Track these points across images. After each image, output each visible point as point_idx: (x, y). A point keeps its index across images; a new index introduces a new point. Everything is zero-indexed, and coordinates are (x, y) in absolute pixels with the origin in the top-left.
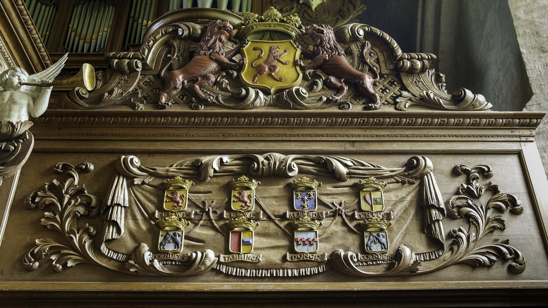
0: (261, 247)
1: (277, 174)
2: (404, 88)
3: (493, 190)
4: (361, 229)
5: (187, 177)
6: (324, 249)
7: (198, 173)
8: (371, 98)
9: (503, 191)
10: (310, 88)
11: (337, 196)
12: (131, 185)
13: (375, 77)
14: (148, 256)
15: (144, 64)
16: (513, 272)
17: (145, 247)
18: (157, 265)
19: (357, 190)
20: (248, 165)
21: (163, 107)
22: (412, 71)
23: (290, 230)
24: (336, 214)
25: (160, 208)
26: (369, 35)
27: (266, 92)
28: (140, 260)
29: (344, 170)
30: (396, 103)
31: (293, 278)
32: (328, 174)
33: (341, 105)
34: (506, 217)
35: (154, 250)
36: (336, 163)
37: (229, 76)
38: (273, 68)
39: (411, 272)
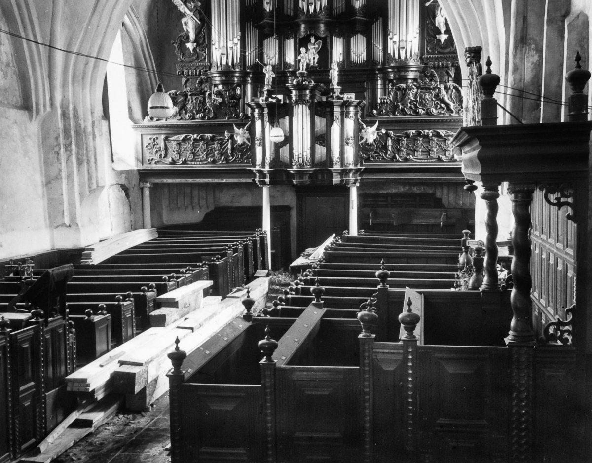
5: (405, 137)
7: (407, 136)
8: (452, 112)
10: (436, 109)
12: (391, 139)
13: (454, 103)
14: (398, 158)
15: (390, 100)
17: (396, 155)
18: (400, 160)
20: (419, 134)
21: (397, 115)
25: (399, 145)
27: (424, 110)
28: (396, 159)
29: (443, 135)
30: (459, 113)
31: (430, 162)
32: (438, 135)
33: (444, 114)
35: (398, 156)
36: (441, 134)
37: (414, 104)
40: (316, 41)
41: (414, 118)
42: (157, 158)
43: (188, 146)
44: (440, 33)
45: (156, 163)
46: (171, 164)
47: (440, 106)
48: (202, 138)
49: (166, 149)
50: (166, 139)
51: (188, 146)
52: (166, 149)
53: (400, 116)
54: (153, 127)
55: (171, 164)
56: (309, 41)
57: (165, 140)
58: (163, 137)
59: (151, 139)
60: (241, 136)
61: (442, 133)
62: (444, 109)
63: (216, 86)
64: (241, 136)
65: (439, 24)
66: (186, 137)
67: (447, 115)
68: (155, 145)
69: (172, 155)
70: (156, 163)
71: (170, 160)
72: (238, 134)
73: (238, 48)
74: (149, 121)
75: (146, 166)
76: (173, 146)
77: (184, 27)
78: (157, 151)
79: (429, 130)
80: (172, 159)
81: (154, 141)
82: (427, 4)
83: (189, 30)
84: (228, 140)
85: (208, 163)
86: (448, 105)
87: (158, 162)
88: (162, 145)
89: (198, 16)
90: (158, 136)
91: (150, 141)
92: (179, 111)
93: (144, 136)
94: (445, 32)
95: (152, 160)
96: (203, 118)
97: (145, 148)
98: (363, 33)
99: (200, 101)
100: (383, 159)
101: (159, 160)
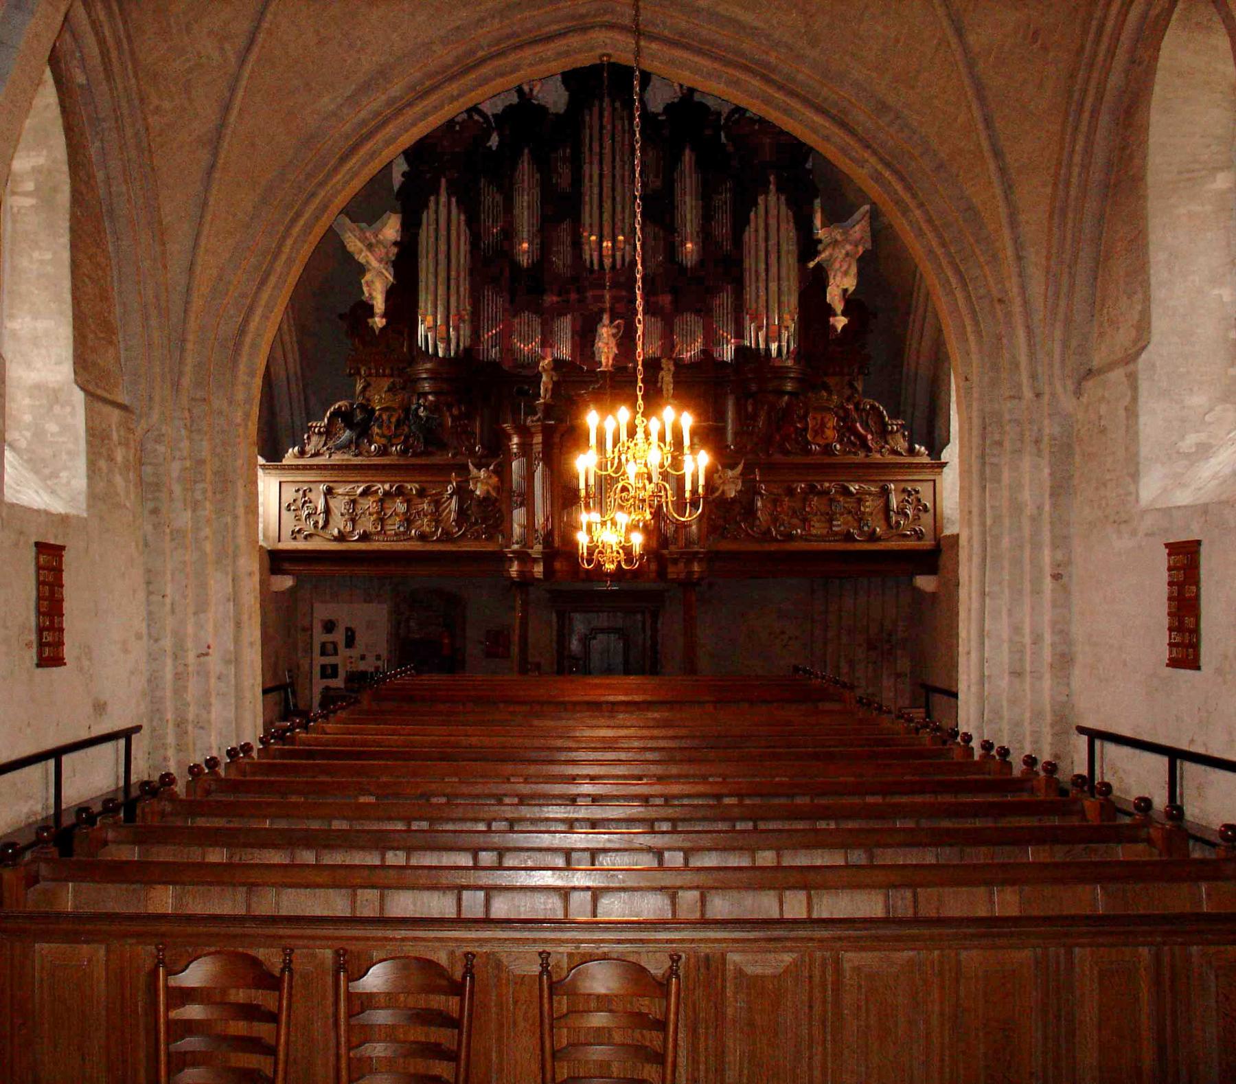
0: (818, 528)
1: (826, 492)
2: (886, 442)
3: (919, 500)
4: (861, 519)
6: (843, 528)
7: (790, 492)
8: (869, 450)
9: (923, 502)
11: (850, 503)
16: (919, 539)
19: (860, 501)
20: (812, 489)
22: (892, 432)
23: (831, 520)
24: (850, 512)
26: (872, 407)
32: (846, 492)
34: (921, 514)
38: (823, 432)
39: (879, 539)
40: (611, 322)
41: (799, 459)
42: (309, 527)
43: (369, 504)
44: (835, 315)
45: (306, 538)
46: (336, 539)
47: (849, 438)
48: (400, 492)
49: (327, 511)
50: (329, 492)
51: (369, 504)
52: (327, 511)
53: (778, 457)
54: (305, 467)
55: (336, 539)
56: (601, 319)
57: (325, 495)
58: (322, 487)
59: (297, 491)
60: (481, 483)
61: (854, 488)
62: (854, 444)
63: (425, 395)
64: (481, 483)
65: (832, 298)
66: (368, 488)
67: (862, 454)
68: (305, 502)
69: (339, 524)
70: (306, 538)
71: (336, 532)
72: (477, 480)
73: (465, 330)
74: (295, 457)
75: (288, 544)
76: (338, 505)
77: (365, 289)
78: (309, 515)
79: (830, 481)
80: (339, 531)
81: (304, 495)
82: (811, 265)
83: (374, 294)
84: (451, 495)
85: (411, 538)
86: (863, 439)
87: (311, 535)
88: (321, 506)
89: (392, 270)
90: (312, 486)
91: (294, 495)
92: (358, 438)
93: (283, 485)
94: (844, 314)
95: (299, 531)
96: (403, 453)
97: (284, 512)
98: (698, 312)
99: (398, 421)
100: (748, 534)
101: (312, 530)
